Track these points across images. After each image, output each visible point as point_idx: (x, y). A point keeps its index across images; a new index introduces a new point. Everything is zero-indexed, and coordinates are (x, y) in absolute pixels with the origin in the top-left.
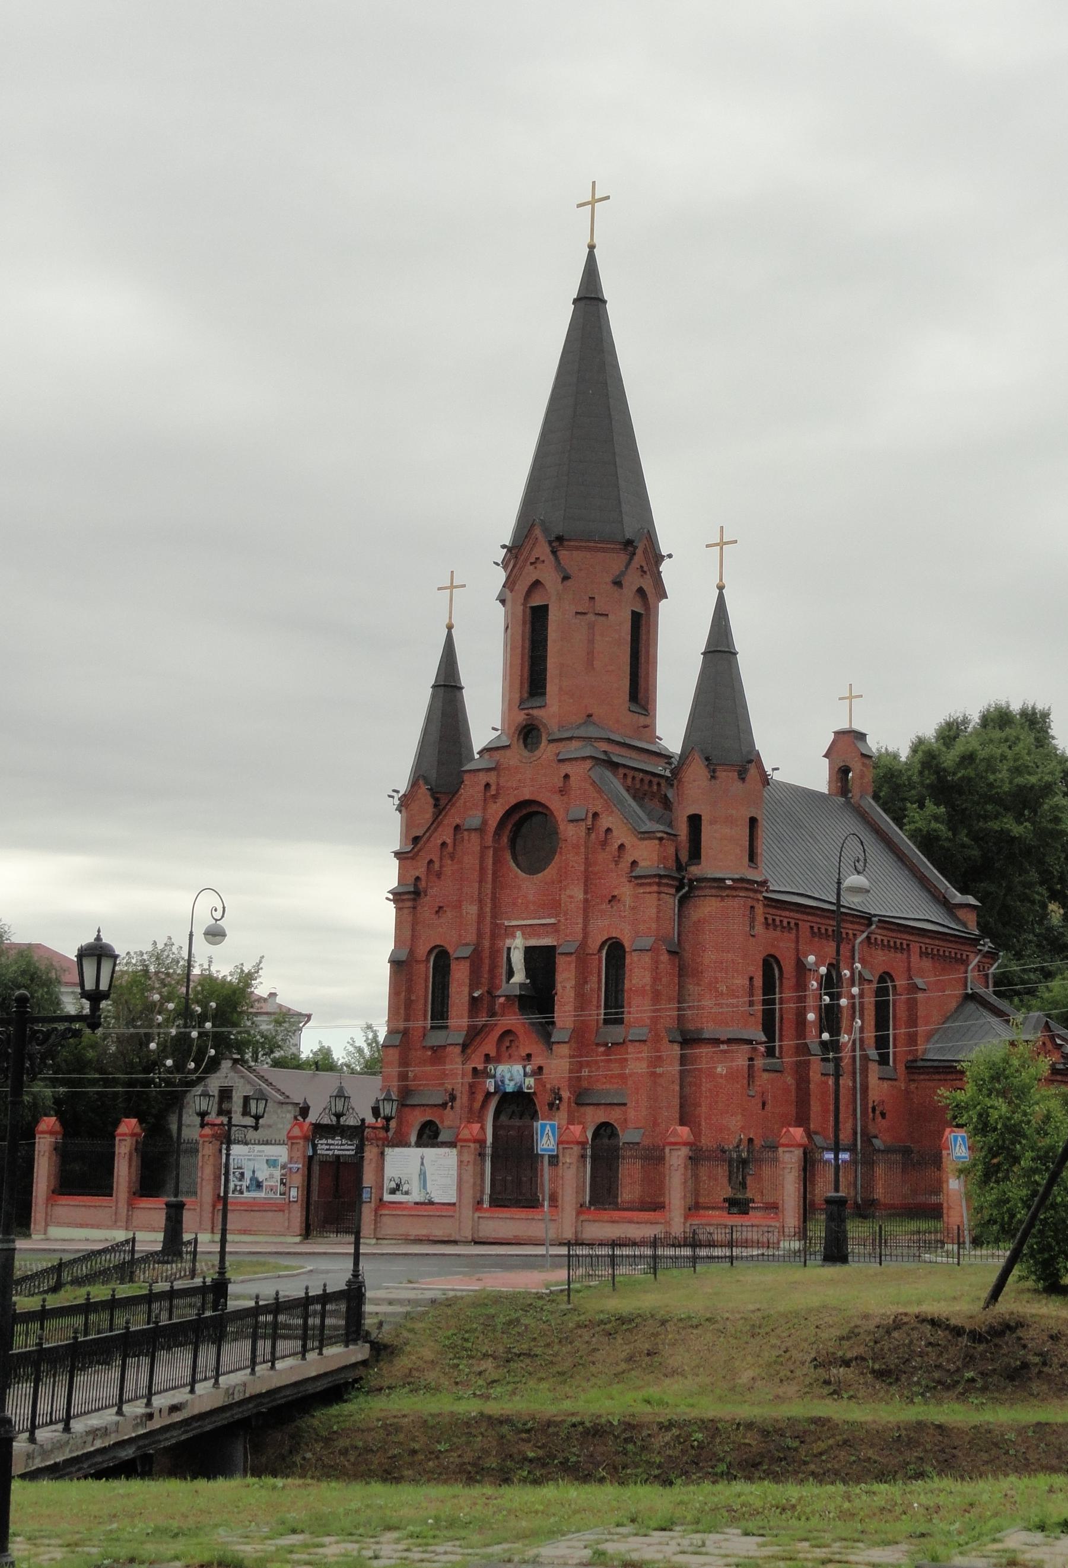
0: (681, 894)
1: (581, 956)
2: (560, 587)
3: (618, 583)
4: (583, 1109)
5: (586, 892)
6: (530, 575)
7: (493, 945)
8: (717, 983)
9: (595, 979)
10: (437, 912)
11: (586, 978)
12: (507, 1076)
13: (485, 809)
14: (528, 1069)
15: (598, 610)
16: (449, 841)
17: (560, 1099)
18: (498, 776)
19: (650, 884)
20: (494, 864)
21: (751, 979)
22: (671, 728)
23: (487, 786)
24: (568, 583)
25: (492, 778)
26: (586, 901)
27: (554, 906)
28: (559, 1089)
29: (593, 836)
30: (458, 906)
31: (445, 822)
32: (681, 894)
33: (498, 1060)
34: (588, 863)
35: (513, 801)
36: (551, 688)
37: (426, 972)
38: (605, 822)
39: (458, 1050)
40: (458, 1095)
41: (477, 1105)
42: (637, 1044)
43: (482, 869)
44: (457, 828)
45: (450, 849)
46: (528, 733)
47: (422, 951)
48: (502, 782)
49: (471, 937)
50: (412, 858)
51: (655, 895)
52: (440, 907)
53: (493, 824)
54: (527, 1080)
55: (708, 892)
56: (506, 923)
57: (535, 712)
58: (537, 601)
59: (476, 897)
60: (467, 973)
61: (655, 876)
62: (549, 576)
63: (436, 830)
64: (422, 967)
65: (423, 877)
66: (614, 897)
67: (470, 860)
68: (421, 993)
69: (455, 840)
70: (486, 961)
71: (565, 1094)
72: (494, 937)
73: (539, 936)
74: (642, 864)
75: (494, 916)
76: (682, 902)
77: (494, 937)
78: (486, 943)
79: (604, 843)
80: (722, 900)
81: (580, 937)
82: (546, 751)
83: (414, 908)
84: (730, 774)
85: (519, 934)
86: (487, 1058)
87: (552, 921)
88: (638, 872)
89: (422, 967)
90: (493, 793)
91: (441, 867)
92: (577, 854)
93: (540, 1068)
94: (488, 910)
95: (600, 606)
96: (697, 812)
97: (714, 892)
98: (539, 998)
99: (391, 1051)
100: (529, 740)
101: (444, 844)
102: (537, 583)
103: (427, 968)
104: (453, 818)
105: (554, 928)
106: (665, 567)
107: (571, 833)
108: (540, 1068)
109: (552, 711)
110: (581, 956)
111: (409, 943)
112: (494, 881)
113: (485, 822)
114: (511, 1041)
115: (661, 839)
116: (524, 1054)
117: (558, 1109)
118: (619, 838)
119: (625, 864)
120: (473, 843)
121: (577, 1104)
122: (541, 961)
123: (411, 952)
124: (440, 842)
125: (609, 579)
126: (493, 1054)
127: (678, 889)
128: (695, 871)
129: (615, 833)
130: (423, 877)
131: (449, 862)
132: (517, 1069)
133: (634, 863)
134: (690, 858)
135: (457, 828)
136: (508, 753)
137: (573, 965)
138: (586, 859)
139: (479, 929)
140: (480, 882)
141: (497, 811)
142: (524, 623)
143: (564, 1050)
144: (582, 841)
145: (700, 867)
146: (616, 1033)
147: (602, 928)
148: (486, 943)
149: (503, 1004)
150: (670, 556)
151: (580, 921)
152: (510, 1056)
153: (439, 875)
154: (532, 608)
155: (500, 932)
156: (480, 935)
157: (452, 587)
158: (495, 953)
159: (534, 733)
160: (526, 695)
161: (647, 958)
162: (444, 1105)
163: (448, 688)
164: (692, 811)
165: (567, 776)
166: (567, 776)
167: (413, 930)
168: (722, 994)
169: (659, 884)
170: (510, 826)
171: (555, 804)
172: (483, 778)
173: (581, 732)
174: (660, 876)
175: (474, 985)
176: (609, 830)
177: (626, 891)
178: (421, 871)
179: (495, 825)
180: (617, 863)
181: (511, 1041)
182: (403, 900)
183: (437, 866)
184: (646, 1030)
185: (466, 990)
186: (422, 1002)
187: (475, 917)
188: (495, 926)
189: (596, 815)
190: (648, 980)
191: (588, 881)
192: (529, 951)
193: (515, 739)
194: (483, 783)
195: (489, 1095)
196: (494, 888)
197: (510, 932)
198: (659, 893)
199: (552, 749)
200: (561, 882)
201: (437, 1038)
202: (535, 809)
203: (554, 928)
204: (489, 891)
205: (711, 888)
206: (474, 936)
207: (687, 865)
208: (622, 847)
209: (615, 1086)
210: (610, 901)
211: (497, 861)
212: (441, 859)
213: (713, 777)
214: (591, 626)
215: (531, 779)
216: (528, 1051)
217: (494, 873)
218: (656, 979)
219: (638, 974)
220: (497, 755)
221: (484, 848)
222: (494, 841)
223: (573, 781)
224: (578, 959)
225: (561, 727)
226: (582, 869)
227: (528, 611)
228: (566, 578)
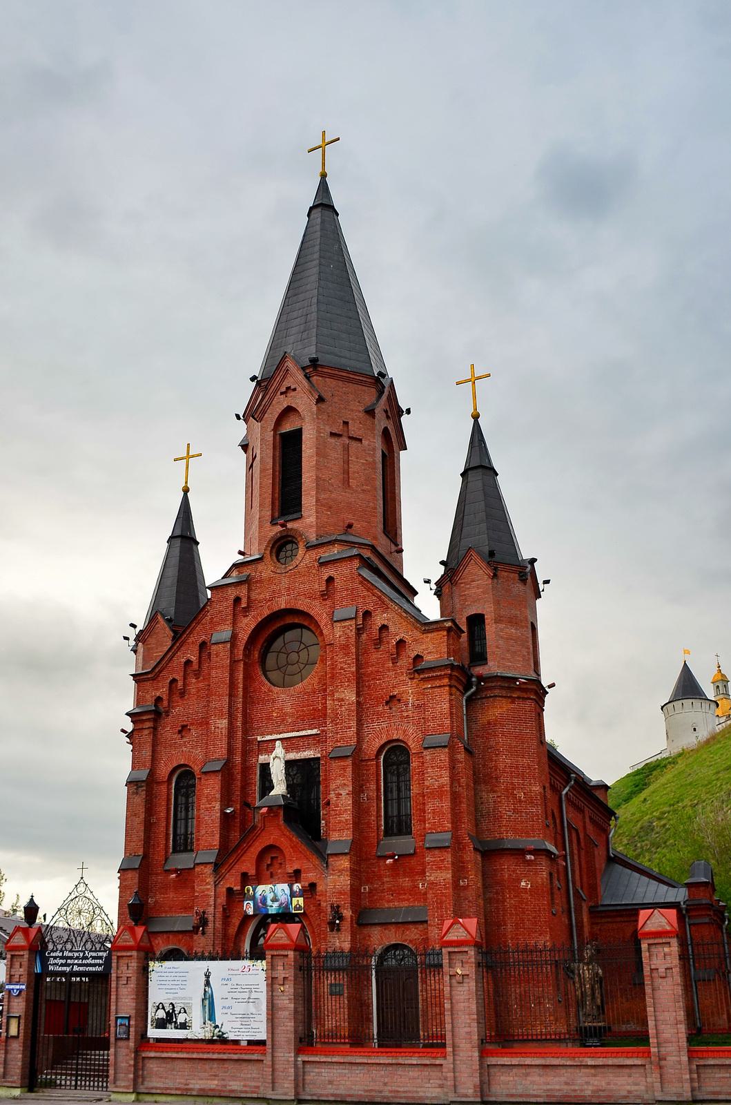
0: (469, 693)
1: (357, 758)
2: (315, 408)
3: (370, 412)
4: (366, 931)
5: (358, 695)
6: (281, 403)
7: (244, 761)
8: (514, 789)
9: (373, 787)
10: (180, 732)
11: (361, 787)
12: (270, 896)
13: (234, 623)
14: (297, 887)
15: (352, 434)
16: (193, 658)
17: (341, 918)
18: (249, 590)
19: (440, 677)
20: (244, 678)
21: (544, 788)
22: (423, 552)
23: (237, 600)
24: (323, 406)
25: (243, 592)
26: (358, 703)
27: (318, 716)
28: (338, 907)
29: (364, 636)
30: (205, 723)
31: (190, 640)
32: (469, 693)
33: (259, 880)
34: (359, 666)
35: (266, 612)
36: (308, 501)
37: (166, 793)
38: (379, 619)
39: (209, 870)
40: (211, 918)
41: (232, 931)
42: (437, 852)
43: (232, 685)
44: (203, 646)
45: (195, 666)
46: (281, 546)
47: (164, 770)
48: (254, 596)
49: (220, 750)
50: (153, 679)
51: (447, 688)
52: (184, 727)
53: (244, 636)
54: (295, 900)
55: (497, 692)
56: (259, 738)
57: (289, 525)
58: (287, 427)
59: (226, 710)
60: (218, 787)
61: (446, 666)
62: (303, 401)
63: (179, 649)
64: (164, 788)
65: (165, 697)
66: (394, 696)
67: (219, 673)
68: (163, 815)
69: (200, 657)
70: (241, 776)
71: (347, 913)
72: (245, 754)
73: (298, 749)
74: (428, 658)
75: (246, 732)
76: (470, 700)
77: (245, 754)
78: (238, 759)
79: (379, 642)
80: (513, 702)
81: (354, 741)
82: (303, 558)
83: (155, 728)
84: (512, 575)
85: (278, 743)
86: (245, 879)
87: (314, 731)
88: (423, 665)
89: (164, 788)
90: (244, 605)
91: (185, 685)
92: (347, 654)
93: (313, 886)
94: (239, 724)
95: (354, 429)
96: (480, 612)
97: (504, 693)
98: (303, 811)
99: (130, 875)
100: (282, 554)
101: (188, 662)
102: (289, 411)
103: (169, 789)
104: (197, 637)
105: (317, 740)
106: (405, 419)
107: (338, 633)
108: (313, 886)
109: (308, 522)
110: (357, 758)
111: (148, 764)
112: (245, 697)
113: (234, 637)
114: (272, 858)
115: (449, 630)
116: (290, 870)
117: (339, 930)
118: (397, 634)
119: (405, 662)
120: (221, 656)
121: (357, 923)
122: (304, 775)
123: (152, 773)
124: (183, 660)
125: (361, 409)
126: (252, 872)
127: (467, 688)
128: (479, 670)
129: (392, 629)
130: (165, 697)
131: (194, 680)
132: (282, 889)
133: (418, 658)
134: (471, 662)
135: (203, 646)
136: (260, 566)
137: (349, 770)
138: (357, 660)
139: (229, 743)
140: (230, 696)
141: (248, 624)
142: (274, 448)
143: (345, 863)
144: (353, 640)
145: (486, 667)
146: (403, 844)
147: (378, 733)
148: (238, 759)
149: (263, 814)
150: (408, 411)
151: (353, 724)
152: (272, 875)
153: (182, 694)
154: (283, 436)
155: (251, 748)
156: (230, 750)
157: (189, 457)
158: (246, 769)
159: (289, 547)
160: (276, 514)
161: (443, 756)
162: (195, 930)
163: (184, 539)
164: (472, 611)
165: (330, 580)
166: (330, 580)
167: (154, 751)
168: (520, 801)
169: (450, 677)
170: (262, 641)
171: (318, 610)
172: (232, 593)
173: (344, 538)
174: (452, 666)
175: (226, 800)
176: (384, 628)
177: (409, 690)
178: (163, 691)
179: (246, 638)
180: (394, 661)
181: (272, 858)
182: (143, 721)
183: (180, 684)
184: (449, 835)
185: (218, 806)
186: (164, 824)
187: (225, 732)
188: (246, 742)
189: (367, 614)
190: (446, 780)
191: (360, 681)
192: (289, 764)
193: (268, 552)
194: (233, 597)
195: (246, 918)
196: (244, 703)
197: (268, 747)
198: (450, 686)
199: (313, 554)
200: (325, 690)
201: (183, 861)
202: (289, 620)
203: (317, 740)
204: (240, 706)
205: (502, 688)
206: (225, 752)
207: (470, 667)
208: (401, 643)
209: (406, 904)
210: (387, 703)
211: (248, 677)
212: (185, 678)
213: (495, 576)
214: (346, 449)
215: (286, 588)
216: (296, 867)
217: (245, 689)
218: (453, 778)
219: (433, 775)
220: (247, 571)
221: (234, 662)
222: (244, 655)
223: (338, 583)
224: (354, 764)
225: (319, 536)
226: (354, 669)
227: (278, 437)
228: (320, 400)
